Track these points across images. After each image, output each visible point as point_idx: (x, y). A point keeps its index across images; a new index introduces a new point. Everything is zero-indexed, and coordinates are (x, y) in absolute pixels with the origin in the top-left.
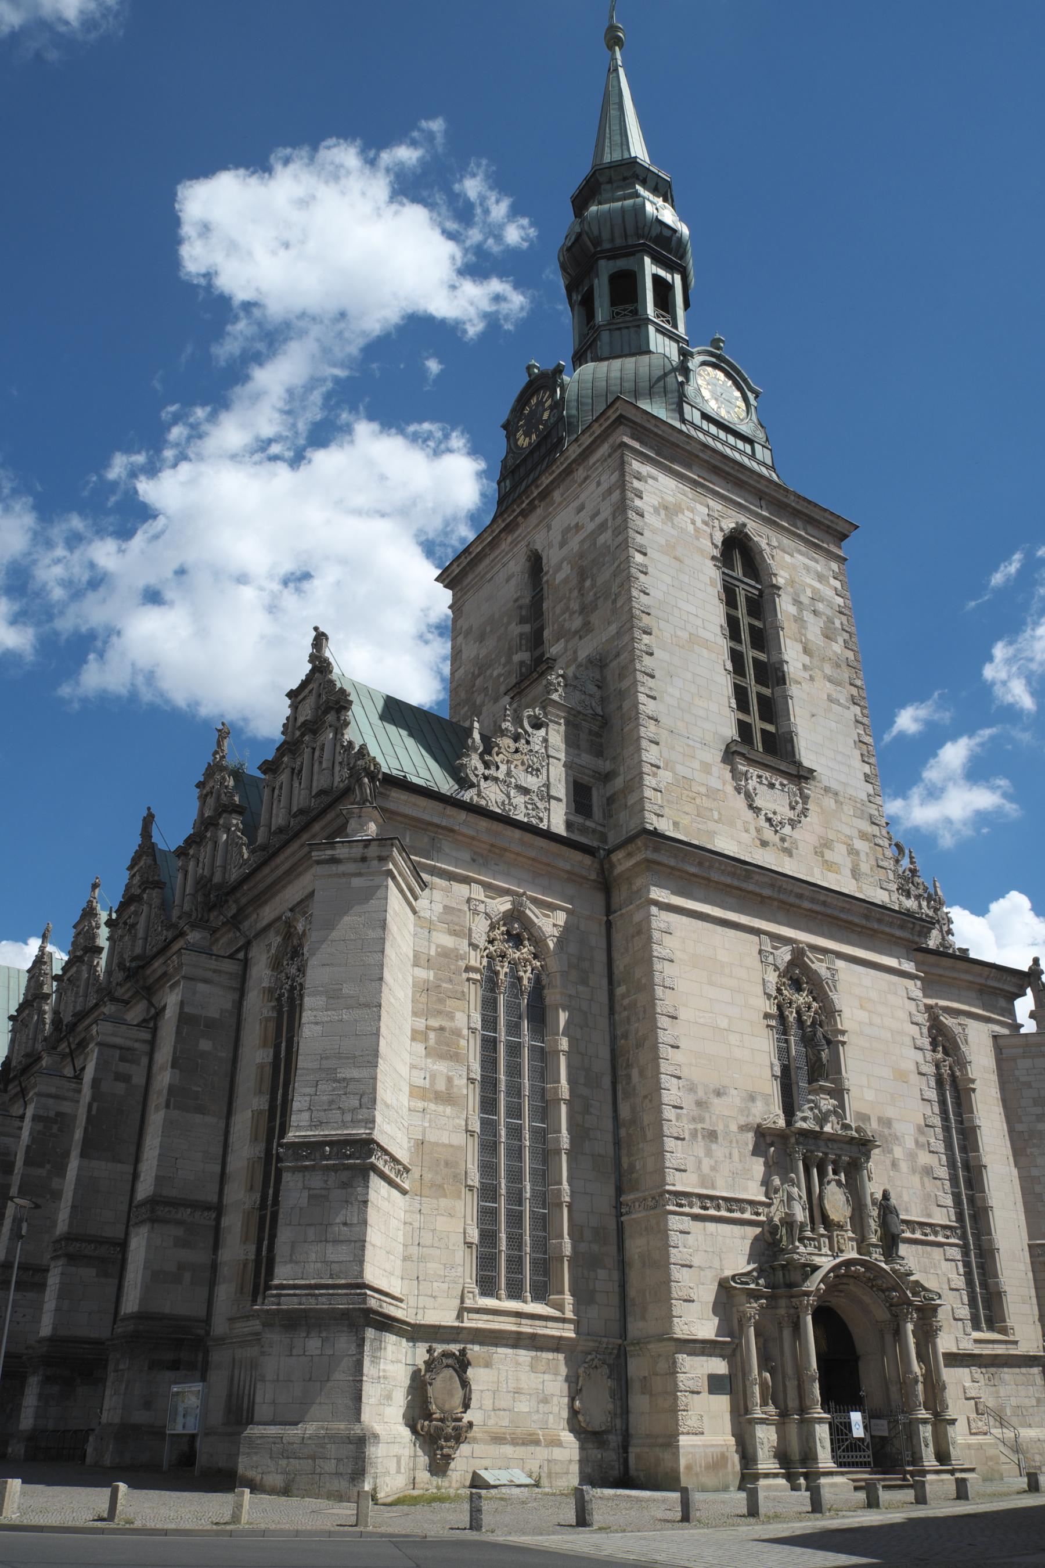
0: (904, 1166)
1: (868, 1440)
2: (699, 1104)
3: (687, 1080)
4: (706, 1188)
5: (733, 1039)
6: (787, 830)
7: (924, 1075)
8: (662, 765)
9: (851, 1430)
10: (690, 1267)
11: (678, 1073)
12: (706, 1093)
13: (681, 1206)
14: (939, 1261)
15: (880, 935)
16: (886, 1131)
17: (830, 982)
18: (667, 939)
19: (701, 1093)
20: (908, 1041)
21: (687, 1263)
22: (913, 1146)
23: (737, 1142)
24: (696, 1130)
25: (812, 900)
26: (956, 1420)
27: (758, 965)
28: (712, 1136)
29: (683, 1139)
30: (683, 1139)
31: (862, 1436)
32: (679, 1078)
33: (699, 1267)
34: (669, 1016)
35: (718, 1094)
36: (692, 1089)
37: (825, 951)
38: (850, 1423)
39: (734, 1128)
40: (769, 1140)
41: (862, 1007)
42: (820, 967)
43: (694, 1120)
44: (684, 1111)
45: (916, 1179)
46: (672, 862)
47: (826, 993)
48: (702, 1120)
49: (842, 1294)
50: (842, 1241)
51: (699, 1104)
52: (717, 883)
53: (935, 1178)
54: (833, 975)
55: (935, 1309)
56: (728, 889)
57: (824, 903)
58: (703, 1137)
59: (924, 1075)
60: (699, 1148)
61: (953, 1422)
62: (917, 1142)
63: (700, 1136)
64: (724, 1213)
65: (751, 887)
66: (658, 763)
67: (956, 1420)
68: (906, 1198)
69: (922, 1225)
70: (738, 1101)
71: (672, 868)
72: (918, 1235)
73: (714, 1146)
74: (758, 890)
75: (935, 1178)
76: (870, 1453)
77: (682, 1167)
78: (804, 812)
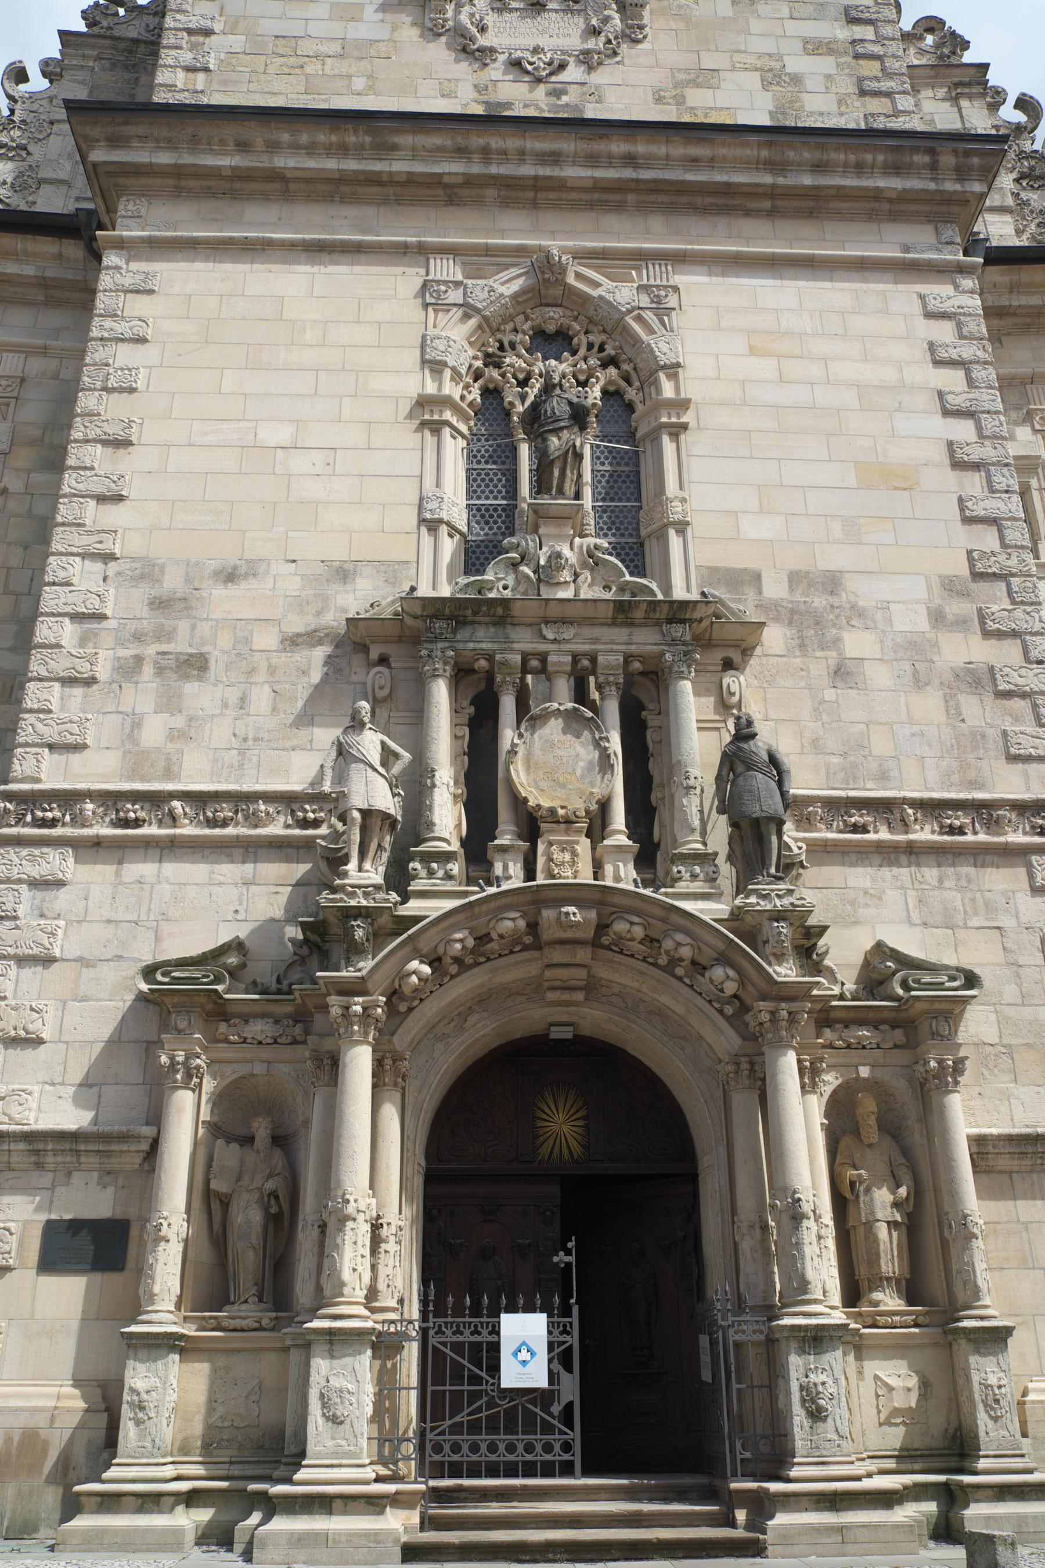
0: (879, 676)
1: (570, 1388)
2: (160, 604)
3: (133, 559)
4: (143, 779)
5: (299, 463)
6: (573, 73)
7: (976, 466)
8: (217, 27)
9: (495, 1368)
10: (48, 961)
11: (107, 546)
12: (188, 580)
13: (53, 823)
14: (1008, 897)
15: (836, 205)
16: (819, 601)
17: (648, 316)
18: (137, 306)
19: (172, 582)
20: (928, 402)
21: (36, 951)
22: (922, 623)
23: (272, 670)
24: (139, 659)
25: (592, 160)
26: (1008, 1331)
27: (413, 311)
28: (195, 665)
29: (91, 681)
30: (91, 681)
31: (543, 1383)
32: (111, 557)
33: (80, 960)
34: (105, 443)
35: (230, 576)
36: (147, 572)
37: (641, 258)
38: (495, 1348)
39: (267, 640)
40: (374, 653)
41: (753, 351)
42: (622, 293)
43: (138, 637)
44: (111, 624)
45: (930, 705)
46: (165, 158)
47: (636, 341)
48: (162, 635)
49: (580, 996)
50: (558, 856)
51: (160, 604)
52: (308, 181)
53: (1008, 695)
54: (658, 300)
55: (948, 1013)
56: (346, 189)
57: (630, 160)
58: (160, 671)
59: (976, 466)
60: (142, 695)
61: (996, 1339)
62: (937, 617)
63: (148, 670)
64: (188, 830)
65: (399, 167)
66: (208, 24)
67: (1008, 1331)
68: (880, 745)
69: (931, 808)
70: (293, 585)
71: (177, 172)
72: (925, 834)
73: (190, 688)
74: (419, 168)
75: (1008, 695)
76: (575, 1435)
77: (70, 739)
78: (633, 35)
